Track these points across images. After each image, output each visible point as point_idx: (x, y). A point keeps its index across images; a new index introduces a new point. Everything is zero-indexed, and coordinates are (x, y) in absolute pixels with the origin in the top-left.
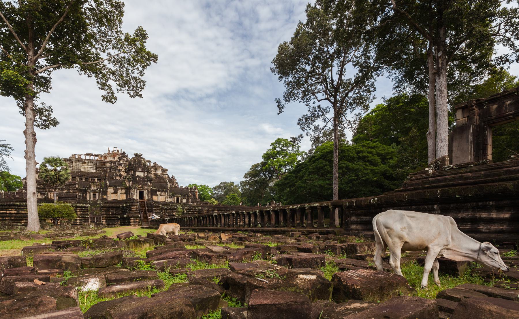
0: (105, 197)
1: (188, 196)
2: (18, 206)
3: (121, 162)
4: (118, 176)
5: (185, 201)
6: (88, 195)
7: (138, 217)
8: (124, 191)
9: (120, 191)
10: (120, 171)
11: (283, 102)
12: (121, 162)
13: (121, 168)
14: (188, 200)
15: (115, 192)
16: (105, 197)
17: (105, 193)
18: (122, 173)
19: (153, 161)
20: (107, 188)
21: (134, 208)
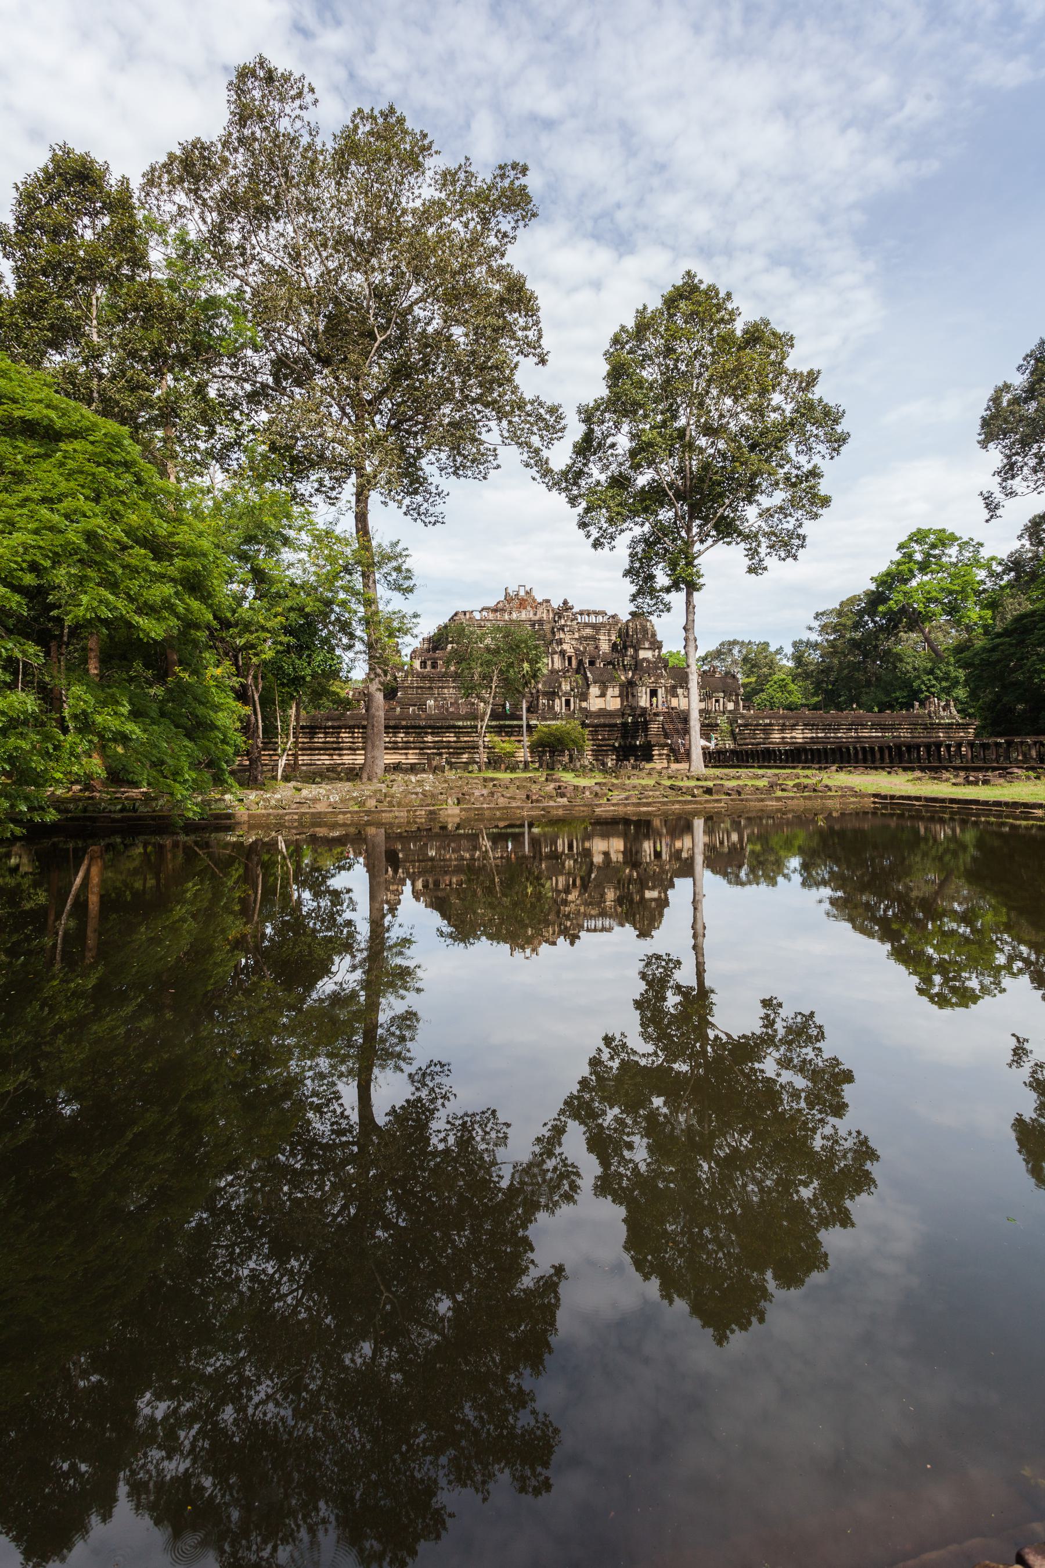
0: (584, 704)
1: (737, 695)
2: (459, 727)
3: (563, 622)
4: (555, 653)
5: (731, 706)
6: (557, 701)
7: (667, 745)
8: (617, 691)
9: (610, 692)
10: (560, 642)
11: (999, 496)
12: (563, 622)
13: (562, 636)
14: (737, 703)
15: (603, 695)
16: (584, 704)
17: (584, 697)
18: (565, 647)
19: (610, 613)
20: (588, 686)
21: (654, 727)
